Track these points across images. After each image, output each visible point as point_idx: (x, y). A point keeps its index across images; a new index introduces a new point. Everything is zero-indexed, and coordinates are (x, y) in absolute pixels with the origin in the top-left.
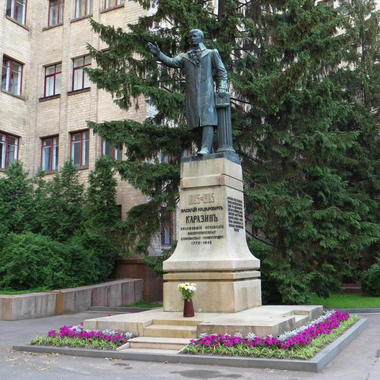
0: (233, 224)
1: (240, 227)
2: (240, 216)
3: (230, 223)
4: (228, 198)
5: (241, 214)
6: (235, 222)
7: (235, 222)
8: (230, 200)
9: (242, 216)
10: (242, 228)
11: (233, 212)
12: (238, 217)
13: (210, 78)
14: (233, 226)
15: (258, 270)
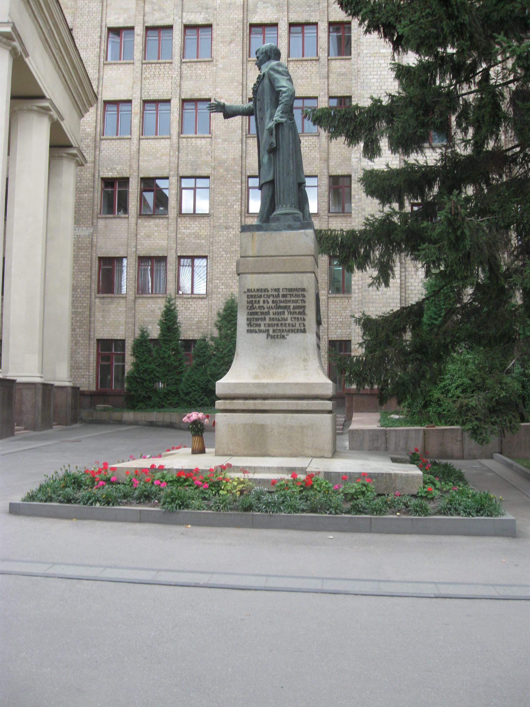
0: (262, 328)
1: (293, 331)
2: (291, 313)
3: (249, 328)
4: (249, 290)
5: (297, 311)
6: (269, 325)
7: (269, 325)
8: (254, 294)
9: (304, 313)
10: (304, 331)
11: (266, 310)
12: (286, 315)
13: (269, 111)
14: (261, 331)
15: (330, 399)
